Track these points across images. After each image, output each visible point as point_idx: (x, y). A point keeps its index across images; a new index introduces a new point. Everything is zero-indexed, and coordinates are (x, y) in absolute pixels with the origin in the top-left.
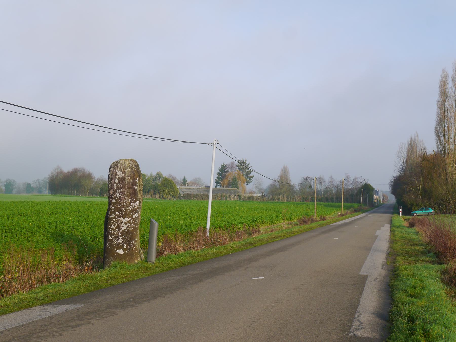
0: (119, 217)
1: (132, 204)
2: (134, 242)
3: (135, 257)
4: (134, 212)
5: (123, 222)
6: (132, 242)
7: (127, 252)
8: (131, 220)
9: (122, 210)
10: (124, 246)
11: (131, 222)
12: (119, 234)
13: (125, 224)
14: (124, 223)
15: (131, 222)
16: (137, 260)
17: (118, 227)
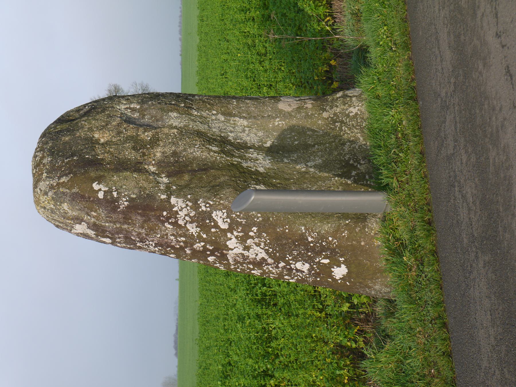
0: (223, 257)
1: (181, 222)
2: (312, 237)
3: (363, 243)
4: (208, 221)
5: (243, 255)
6: (310, 243)
7: (342, 259)
8: (235, 233)
9: (202, 249)
10: (321, 261)
11: (241, 234)
12: (280, 265)
13: (247, 248)
14: (246, 252)
15: (241, 234)
16: (373, 237)
17: (259, 264)
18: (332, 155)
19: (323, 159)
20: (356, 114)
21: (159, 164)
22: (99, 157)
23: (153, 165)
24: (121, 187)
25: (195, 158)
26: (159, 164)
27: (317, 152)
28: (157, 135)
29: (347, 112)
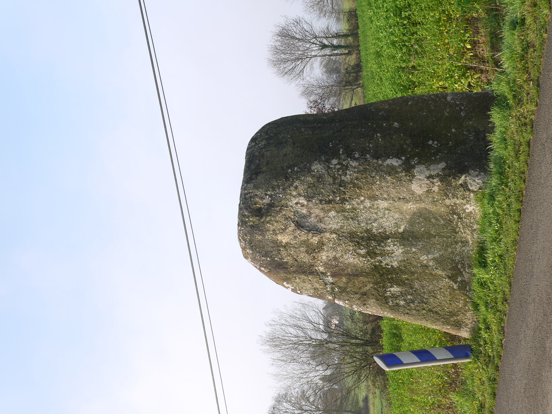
18: (447, 252)
19: (440, 253)
20: (471, 212)
21: (325, 265)
22: (284, 261)
23: (321, 266)
24: (302, 288)
25: (349, 264)
26: (325, 265)
27: (437, 244)
28: (322, 239)
29: (464, 208)
